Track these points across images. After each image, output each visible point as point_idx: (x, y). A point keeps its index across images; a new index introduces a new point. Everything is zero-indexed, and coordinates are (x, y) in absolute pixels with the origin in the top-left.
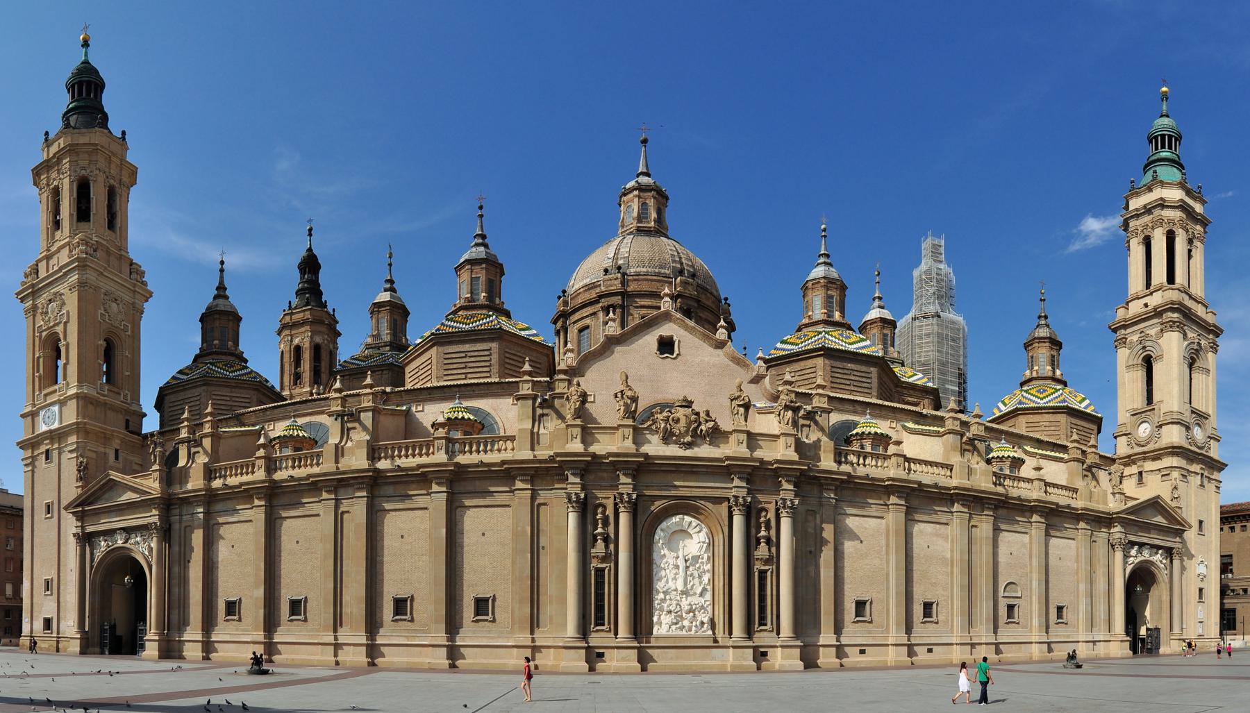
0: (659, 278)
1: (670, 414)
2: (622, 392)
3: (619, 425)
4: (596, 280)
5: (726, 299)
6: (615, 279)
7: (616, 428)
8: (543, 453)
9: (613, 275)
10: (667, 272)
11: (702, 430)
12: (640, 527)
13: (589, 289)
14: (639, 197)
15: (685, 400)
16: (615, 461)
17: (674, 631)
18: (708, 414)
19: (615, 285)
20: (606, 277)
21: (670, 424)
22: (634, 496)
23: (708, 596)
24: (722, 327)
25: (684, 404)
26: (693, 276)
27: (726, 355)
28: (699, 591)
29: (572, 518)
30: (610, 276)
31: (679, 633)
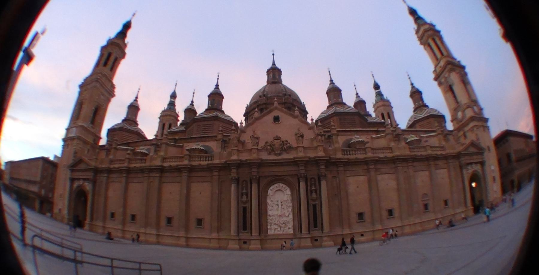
1: (271, 143)
2: (253, 135)
5: (303, 103)
8: (223, 161)
11: (284, 148)
12: (261, 189)
14: (272, 72)
15: (277, 137)
17: (276, 232)
18: (287, 141)
22: (258, 177)
23: (291, 216)
24: (297, 110)
25: (276, 138)
26: (290, 95)
27: (299, 120)
28: (287, 214)
29: (233, 187)
31: (279, 233)
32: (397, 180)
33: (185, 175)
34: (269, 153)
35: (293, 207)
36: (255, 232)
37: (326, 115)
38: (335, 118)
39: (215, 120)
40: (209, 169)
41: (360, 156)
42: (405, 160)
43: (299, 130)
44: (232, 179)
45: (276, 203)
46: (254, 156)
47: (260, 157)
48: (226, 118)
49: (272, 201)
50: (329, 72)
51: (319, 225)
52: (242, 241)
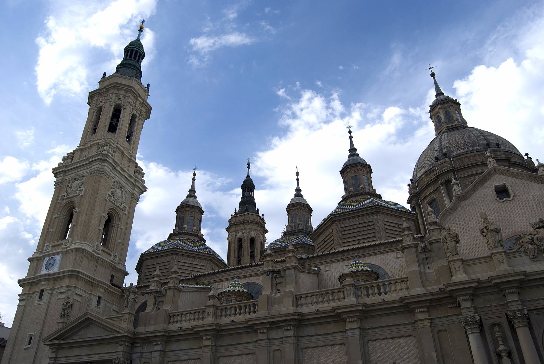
0: (474, 153)
1: (533, 236)
2: (486, 227)
3: (492, 254)
4: (431, 167)
5: (527, 154)
6: (445, 162)
7: (491, 256)
8: (434, 288)
9: (443, 160)
10: (479, 148)
13: (429, 174)
16: (498, 283)
19: (446, 166)
20: (439, 162)
21: (535, 244)
26: (498, 145)
29: (473, 340)
30: (440, 161)
39: (374, 213)
47: (474, 277)
48: (394, 207)
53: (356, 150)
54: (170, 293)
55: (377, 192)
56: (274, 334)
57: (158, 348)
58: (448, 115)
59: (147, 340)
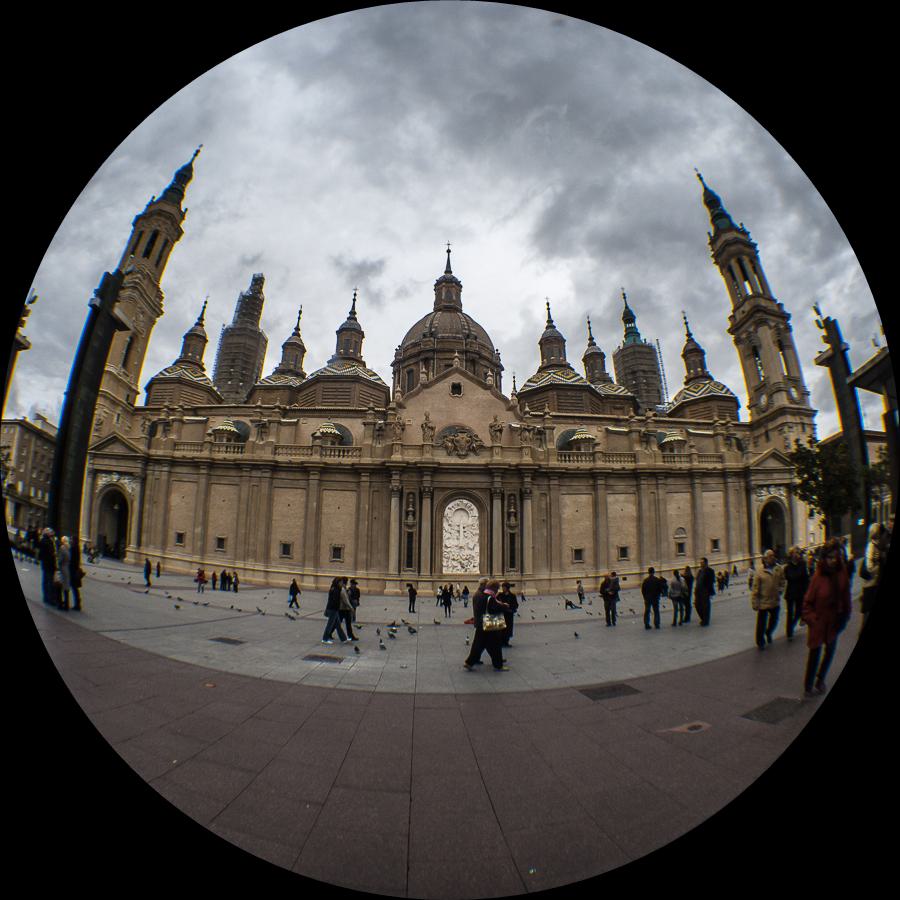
8: (378, 460)
12: (435, 508)
23: (477, 549)
26: (476, 338)
29: (394, 501)
32: (639, 504)
33: (314, 477)
34: (449, 454)
35: (481, 535)
36: (425, 571)
37: (535, 385)
38: (550, 393)
40: (356, 471)
41: (585, 465)
42: (654, 475)
43: (496, 420)
44: (393, 490)
45: (456, 528)
46: (427, 457)
49: (450, 525)
50: (548, 304)
51: (518, 562)
52: (405, 583)
53: (355, 313)
54: (176, 425)
55: (363, 359)
56: (254, 473)
57: (166, 469)
58: (448, 292)
59: (158, 461)
